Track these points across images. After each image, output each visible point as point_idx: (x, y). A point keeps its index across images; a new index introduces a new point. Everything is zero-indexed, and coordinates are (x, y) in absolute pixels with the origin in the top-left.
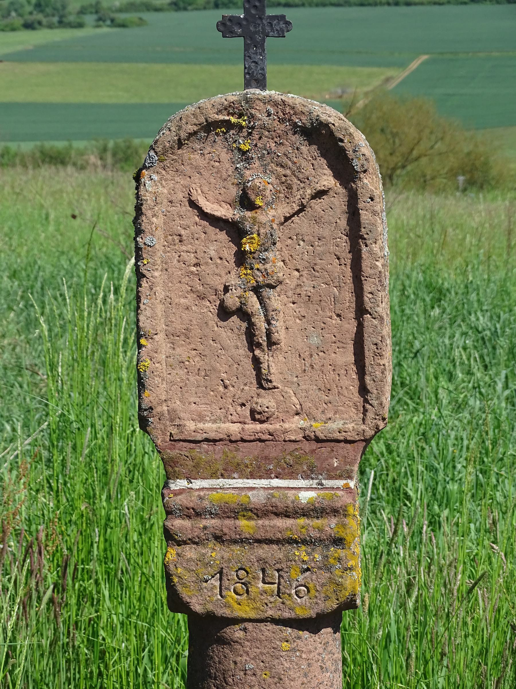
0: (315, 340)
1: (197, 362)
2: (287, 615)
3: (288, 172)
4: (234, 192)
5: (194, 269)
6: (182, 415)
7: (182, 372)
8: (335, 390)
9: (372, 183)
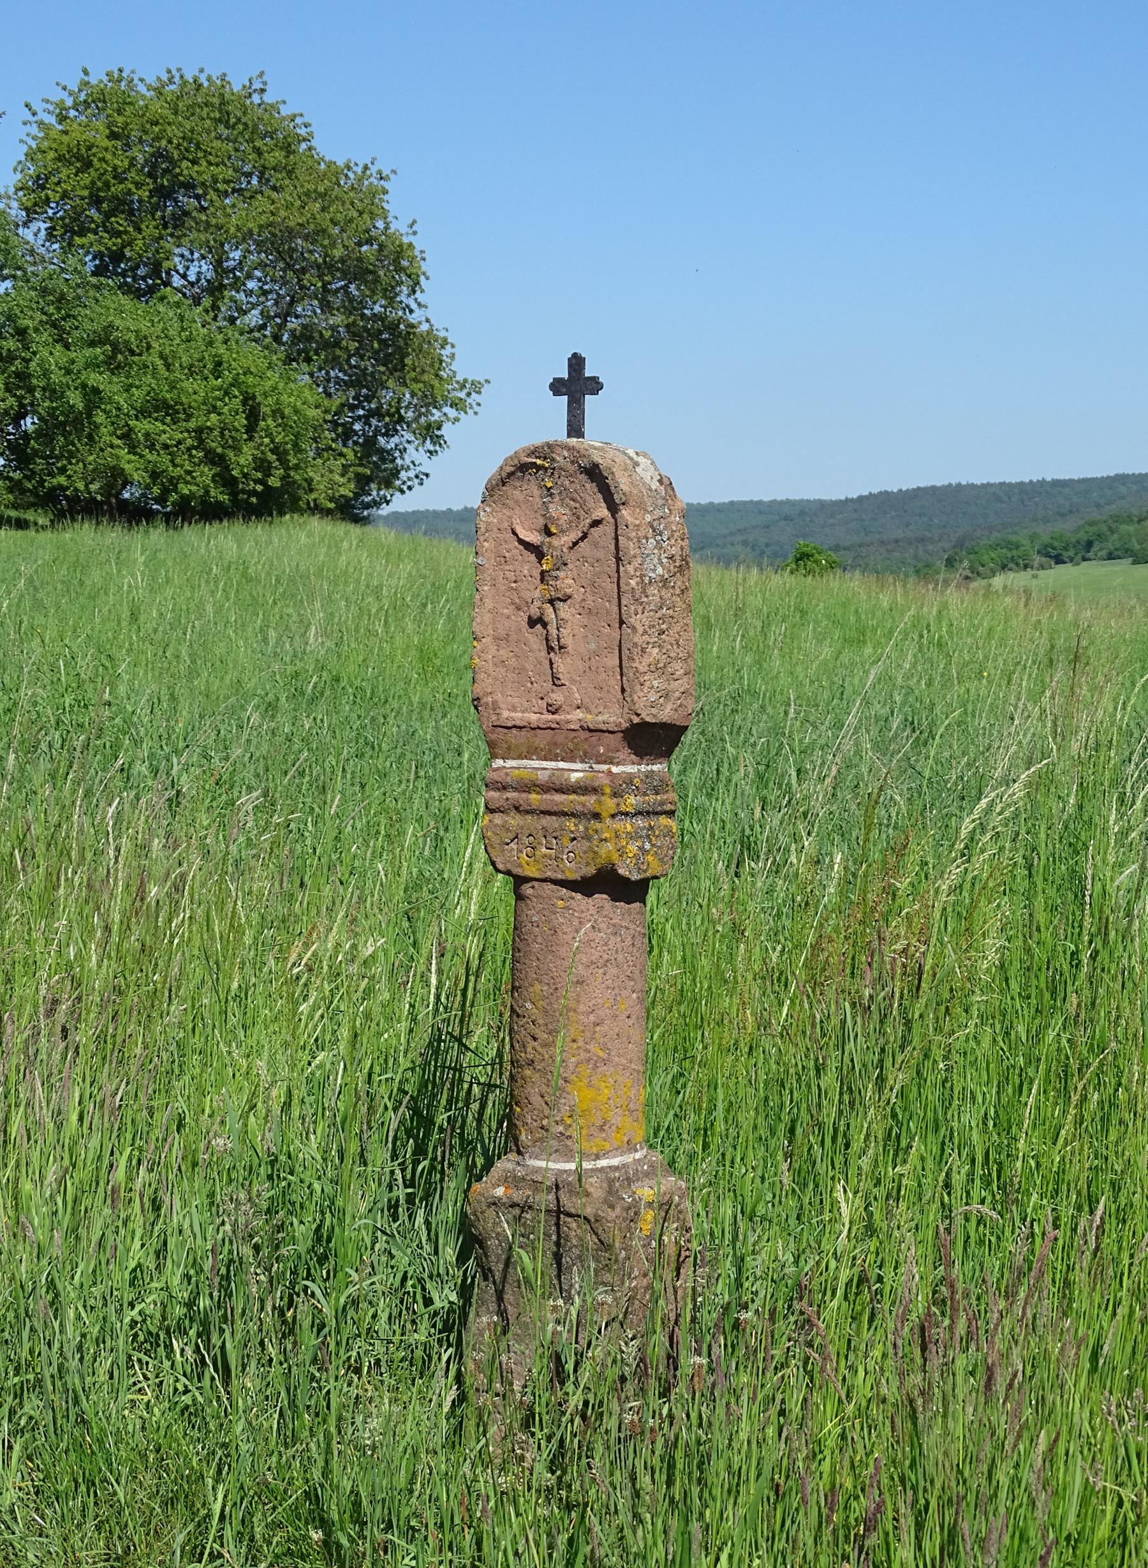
0: (593, 646)
1: (512, 662)
2: (560, 876)
3: (577, 505)
4: (541, 522)
5: (514, 585)
6: (502, 706)
7: (503, 670)
8: (605, 689)
9: (632, 514)
